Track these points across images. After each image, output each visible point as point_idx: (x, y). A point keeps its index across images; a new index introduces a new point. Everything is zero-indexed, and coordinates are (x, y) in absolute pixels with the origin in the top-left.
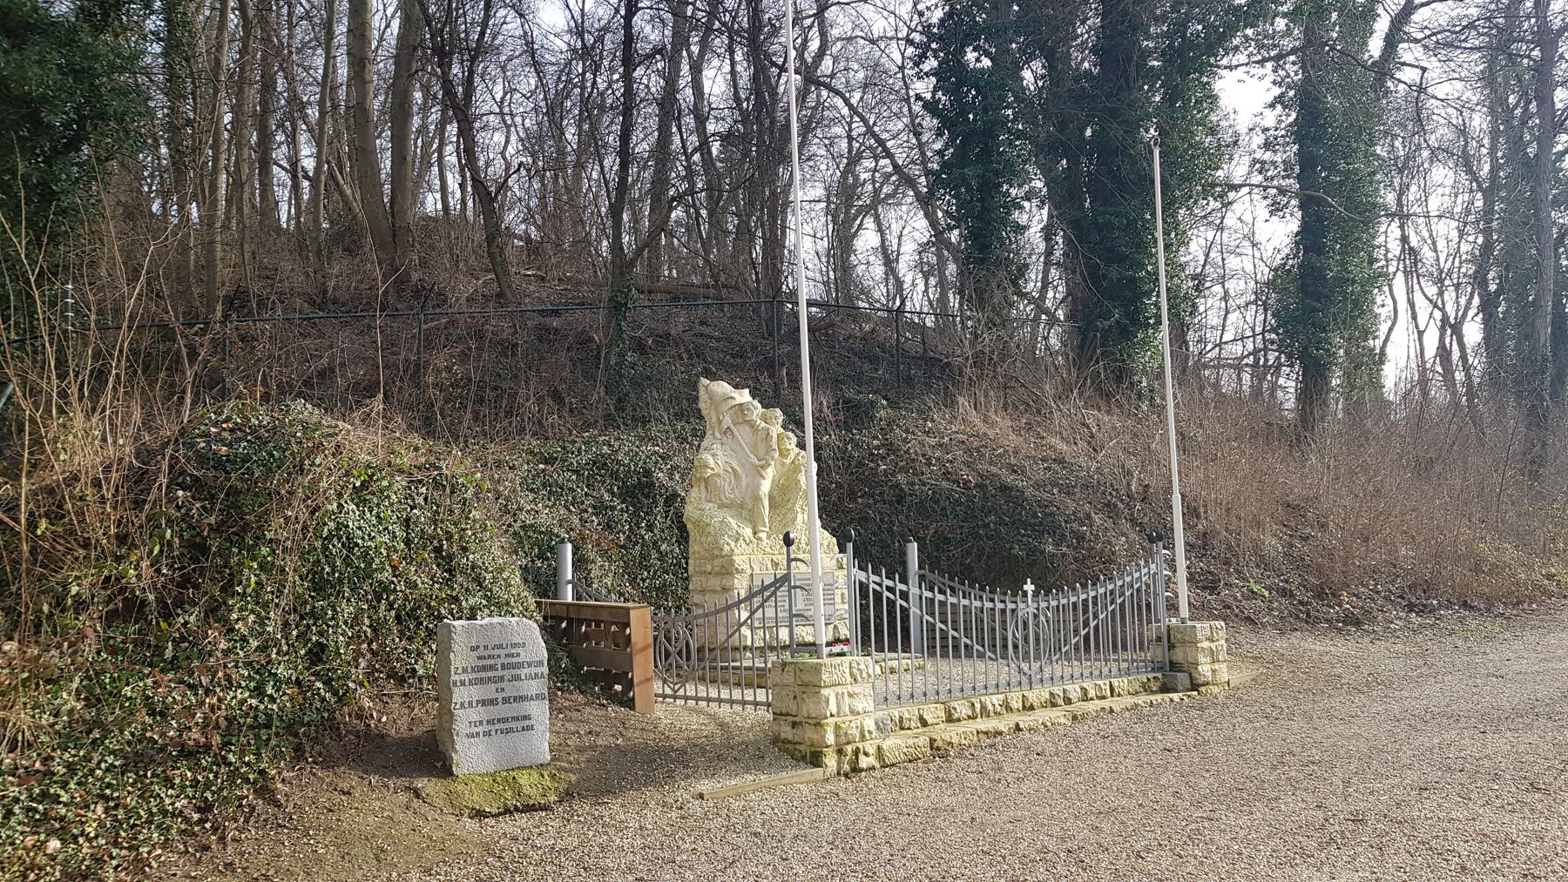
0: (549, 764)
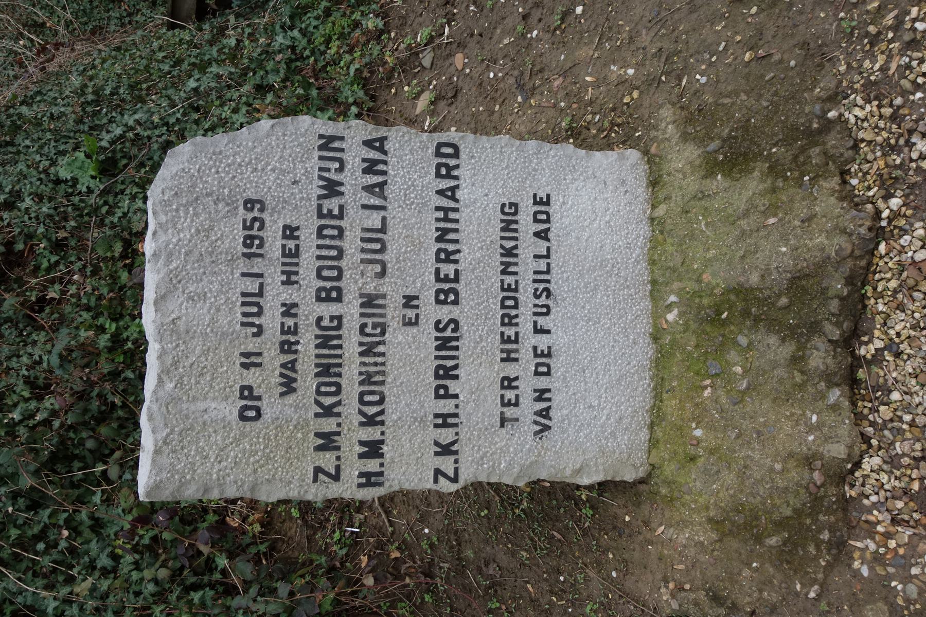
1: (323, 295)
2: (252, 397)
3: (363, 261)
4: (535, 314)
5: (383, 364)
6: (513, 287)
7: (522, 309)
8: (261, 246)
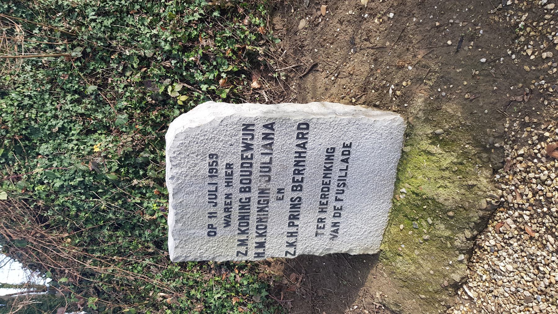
0: (410, 126)
1: (243, 190)
2: (212, 228)
3: (260, 176)
4: (337, 193)
5: (267, 215)
6: (328, 183)
7: (331, 191)
8: (216, 172)
